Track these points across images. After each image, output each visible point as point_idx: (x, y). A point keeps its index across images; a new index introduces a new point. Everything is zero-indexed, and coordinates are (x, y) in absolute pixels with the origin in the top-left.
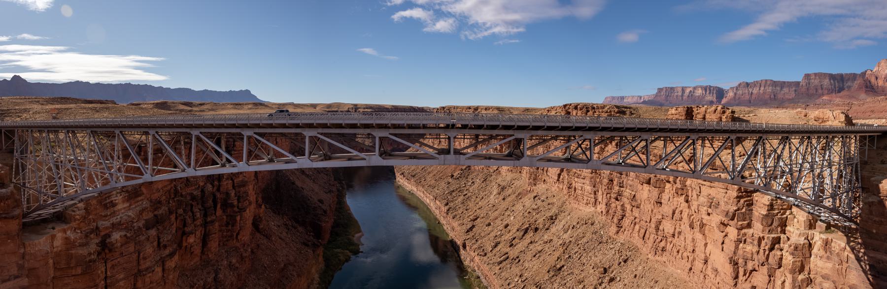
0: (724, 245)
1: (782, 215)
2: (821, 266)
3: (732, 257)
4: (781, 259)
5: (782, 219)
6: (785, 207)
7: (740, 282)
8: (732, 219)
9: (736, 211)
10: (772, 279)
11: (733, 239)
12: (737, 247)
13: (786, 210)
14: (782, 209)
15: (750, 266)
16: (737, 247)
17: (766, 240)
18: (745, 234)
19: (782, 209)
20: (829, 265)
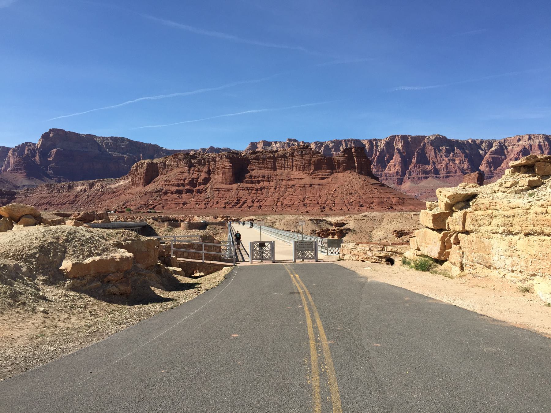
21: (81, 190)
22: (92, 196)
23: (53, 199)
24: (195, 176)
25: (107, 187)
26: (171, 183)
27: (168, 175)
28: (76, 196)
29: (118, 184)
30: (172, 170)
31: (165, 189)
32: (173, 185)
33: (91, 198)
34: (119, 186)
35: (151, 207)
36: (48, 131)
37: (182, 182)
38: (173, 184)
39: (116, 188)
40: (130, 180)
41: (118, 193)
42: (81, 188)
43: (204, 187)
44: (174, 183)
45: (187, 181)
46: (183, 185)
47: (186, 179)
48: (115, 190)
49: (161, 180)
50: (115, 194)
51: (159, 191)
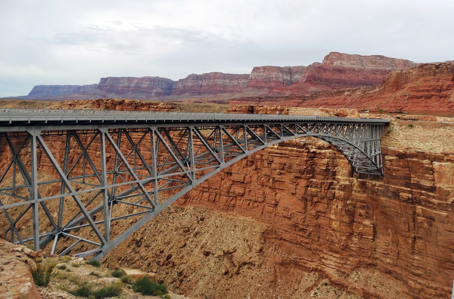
0: (297, 191)
1: (333, 169)
2: (359, 196)
3: (303, 196)
4: (335, 194)
5: (333, 172)
6: (335, 165)
7: (308, 210)
8: (303, 174)
9: (305, 168)
10: (329, 206)
11: (303, 186)
12: (306, 190)
13: (335, 167)
14: (333, 166)
15: (315, 199)
16: (306, 190)
17: (325, 184)
18: (311, 182)
19: (333, 166)
20: (365, 195)
21: (348, 95)
22: (355, 100)
23: (329, 101)
24: (440, 83)
25: (366, 93)
26: (416, 90)
27: (415, 82)
28: (345, 99)
29: (374, 91)
30: (418, 78)
31: (411, 94)
32: (418, 91)
33: (354, 101)
34: (375, 93)
35: (399, 108)
36: (328, 54)
37: (427, 88)
38: (419, 90)
39: (372, 93)
40: (383, 87)
41: (374, 97)
42: (348, 93)
43: (448, 93)
44: (419, 89)
45: (432, 88)
46: (428, 91)
47: (430, 86)
48: (372, 95)
49: (408, 87)
50: (372, 98)
51: (406, 96)
